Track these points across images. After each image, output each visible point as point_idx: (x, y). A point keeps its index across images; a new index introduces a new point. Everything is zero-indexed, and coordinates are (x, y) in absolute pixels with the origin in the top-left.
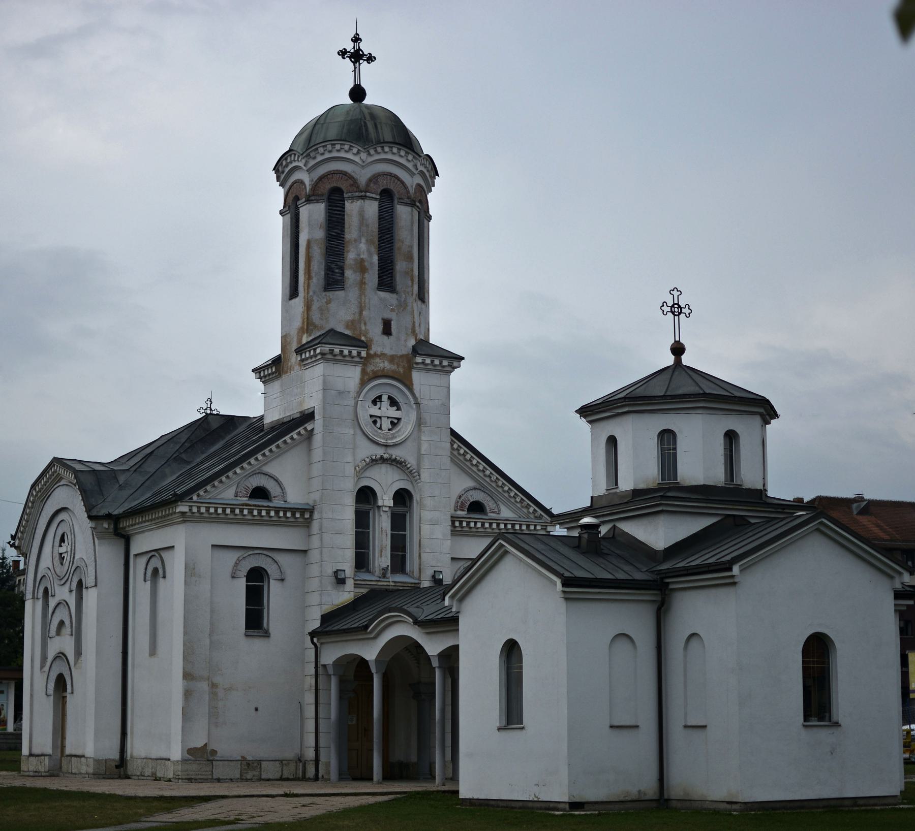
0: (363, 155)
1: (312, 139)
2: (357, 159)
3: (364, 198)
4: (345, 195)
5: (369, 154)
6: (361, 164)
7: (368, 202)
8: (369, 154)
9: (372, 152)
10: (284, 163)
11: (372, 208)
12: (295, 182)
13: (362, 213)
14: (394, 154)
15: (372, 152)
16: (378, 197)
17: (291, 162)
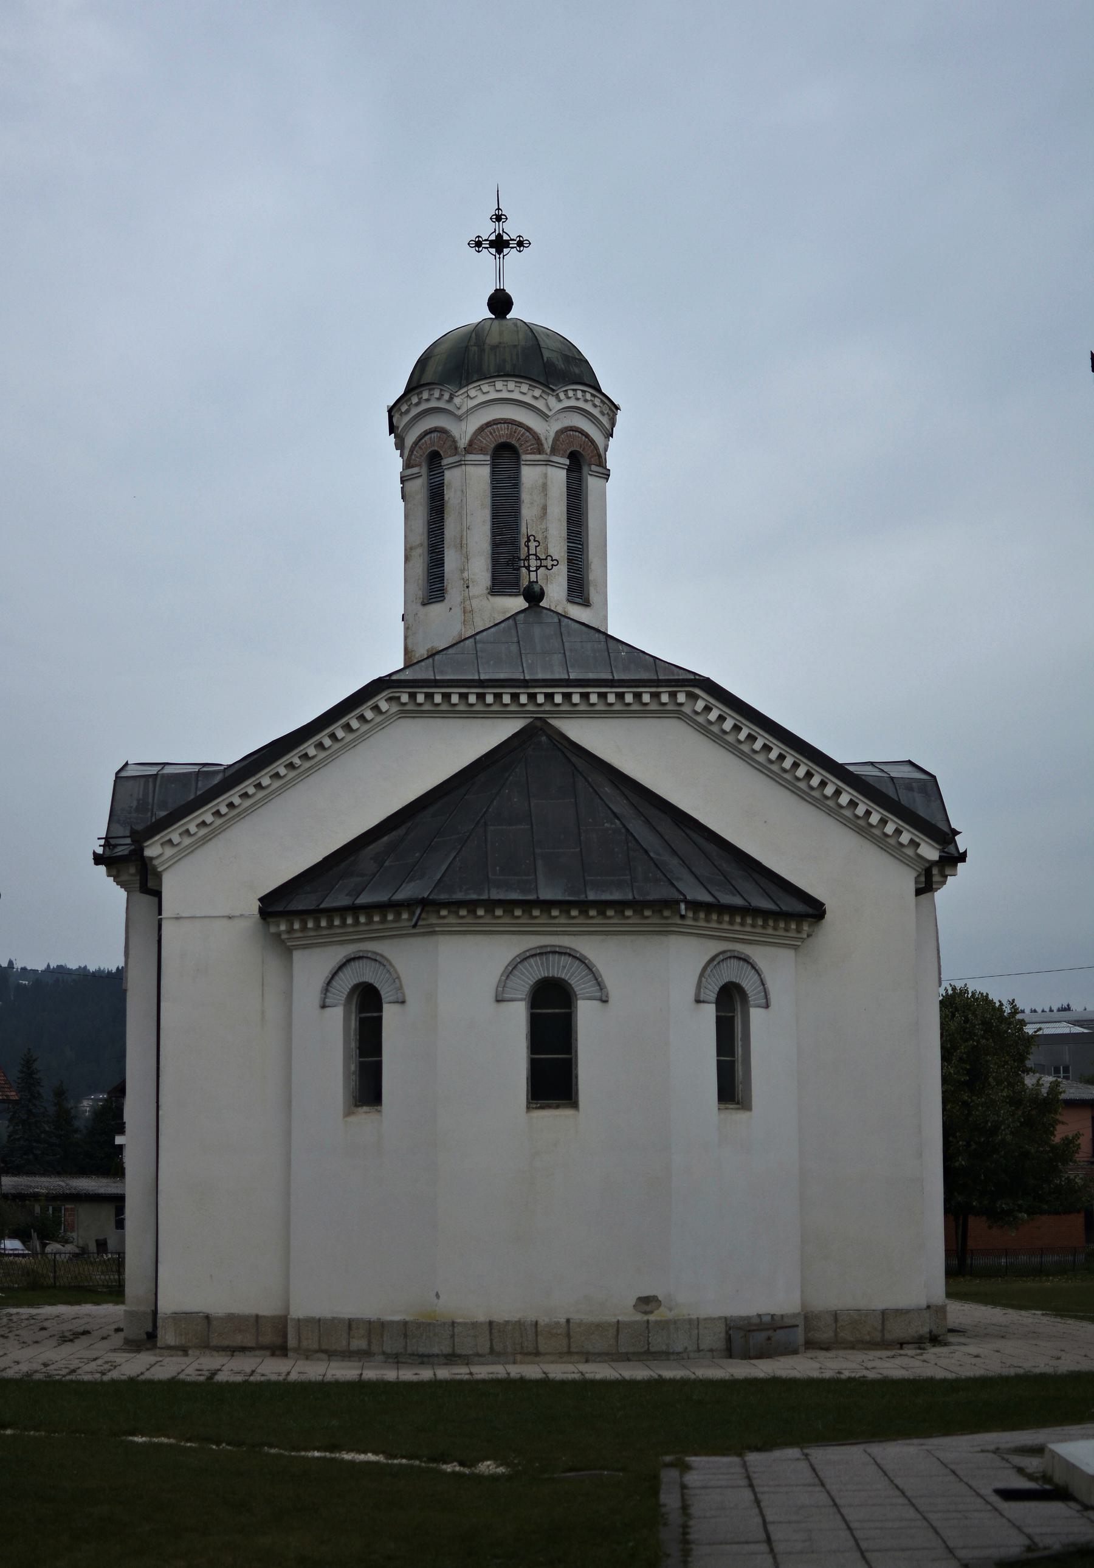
0: (552, 401)
1: (452, 365)
2: (540, 404)
3: (548, 463)
4: (524, 457)
5: (560, 401)
6: (545, 415)
7: (551, 471)
8: (560, 401)
9: (562, 396)
10: (415, 400)
11: (558, 477)
12: (435, 430)
13: (543, 483)
14: (578, 399)
15: (562, 396)
16: (567, 462)
17: (428, 400)
